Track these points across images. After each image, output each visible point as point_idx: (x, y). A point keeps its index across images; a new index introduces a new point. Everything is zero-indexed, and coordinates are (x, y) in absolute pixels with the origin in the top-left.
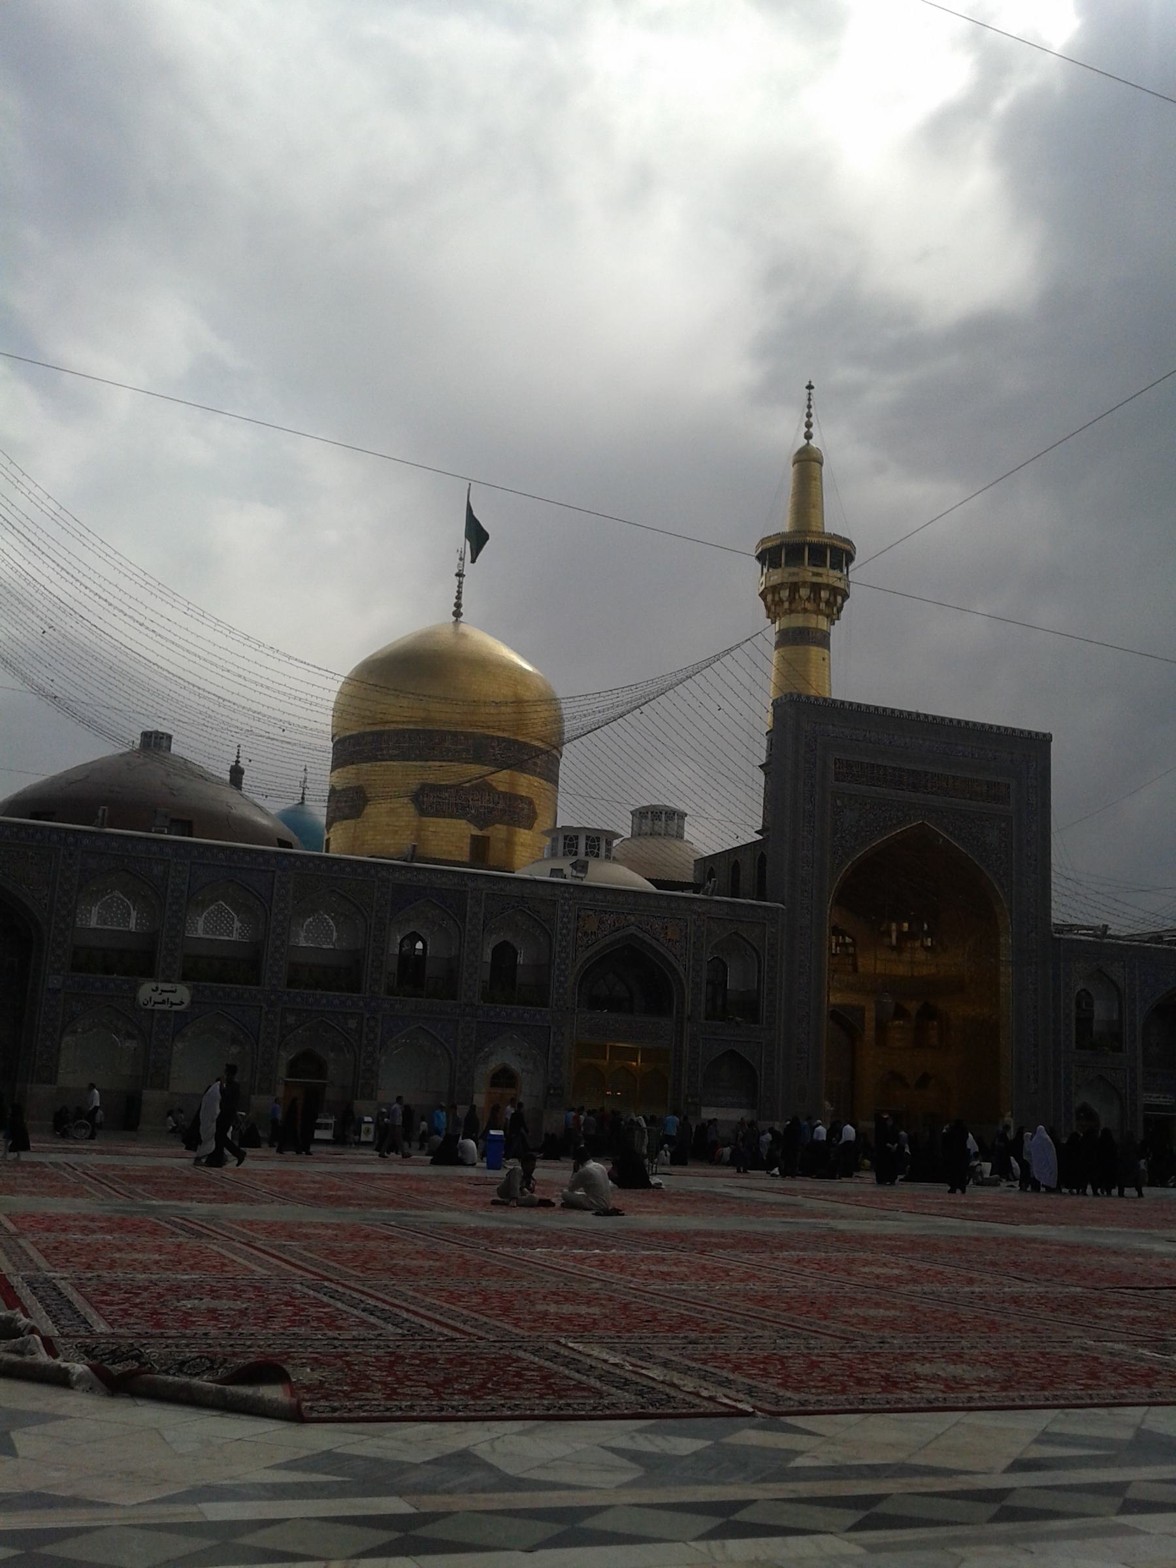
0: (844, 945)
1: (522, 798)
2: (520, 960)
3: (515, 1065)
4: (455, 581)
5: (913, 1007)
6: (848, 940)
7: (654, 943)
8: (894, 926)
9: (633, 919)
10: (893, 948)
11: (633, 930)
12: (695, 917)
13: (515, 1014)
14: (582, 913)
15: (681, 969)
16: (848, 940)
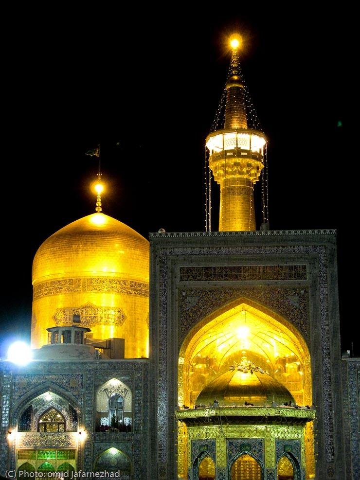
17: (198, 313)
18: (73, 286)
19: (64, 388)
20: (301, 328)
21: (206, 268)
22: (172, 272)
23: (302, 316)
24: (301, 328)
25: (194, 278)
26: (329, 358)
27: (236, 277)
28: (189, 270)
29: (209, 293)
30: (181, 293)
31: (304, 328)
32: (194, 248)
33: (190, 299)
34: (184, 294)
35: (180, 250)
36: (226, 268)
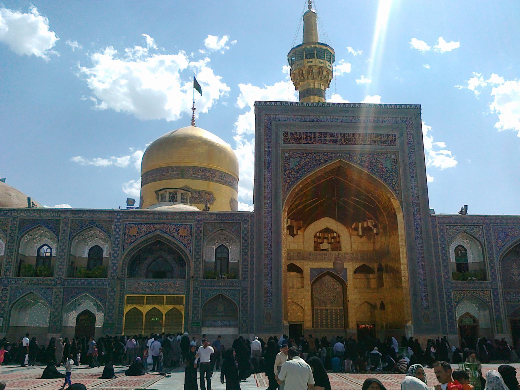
0: (334, 238)
1: (206, 192)
2: (105, 254)
3: (93, 310)
4: (192, 111)
5: (375, 266)
6: (335, 235)
7: (171, 238)
8: (360, 224)
9: (158, 227)
10: (361, 237)
11: (158, 232)
12: (197, 222)
13: (86, 283)
14: (128, 226)
15: (188, 252)
16: (335, 235)
17: (300, 172)
18: (174, 173)
19: (173, 237)
20: (393, 188)
21: (307, 133)
22: (276, 134)
23: (394, 177)
24: (393, 188)
25: (297, 141)
26: (419, 214)
27: (334, 142)
28: (291, 134)
29: (310, 155)
30: (284, 154)
31: (396, 188)
32: (296, 115)
33: (292, 160)
34: (287, 155)
35: (283, 116)
36: (324, 133)
